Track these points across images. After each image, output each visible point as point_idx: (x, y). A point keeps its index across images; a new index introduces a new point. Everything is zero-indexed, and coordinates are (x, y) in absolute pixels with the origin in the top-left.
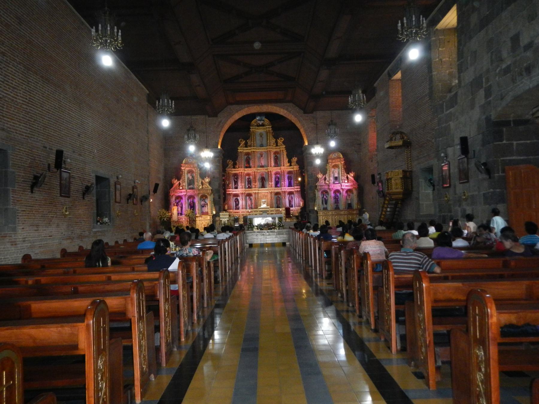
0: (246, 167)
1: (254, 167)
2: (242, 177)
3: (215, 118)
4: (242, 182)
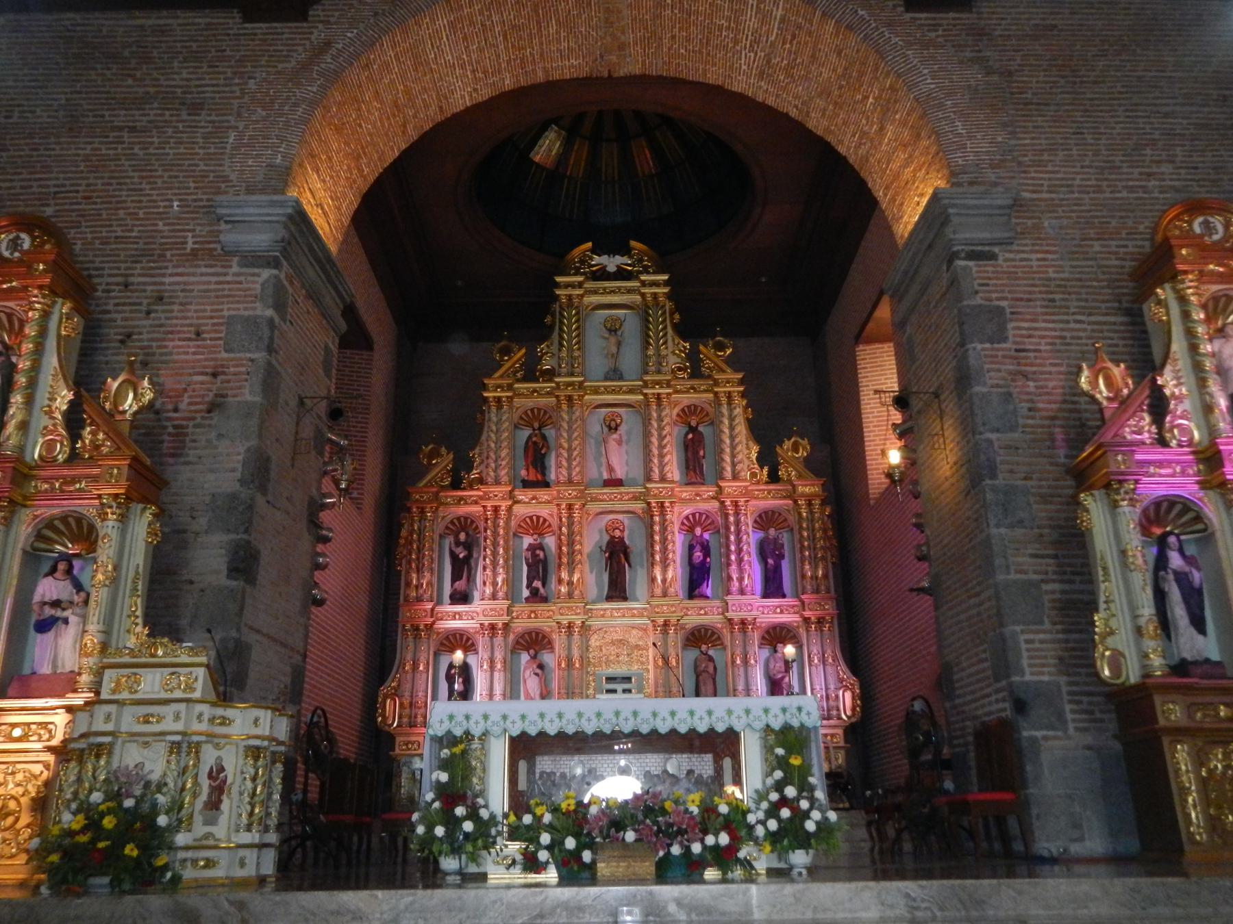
0: (527, 484)
1: (570, 482)
2: (495, 534)
3: (286, 29)
4: (495, 564)
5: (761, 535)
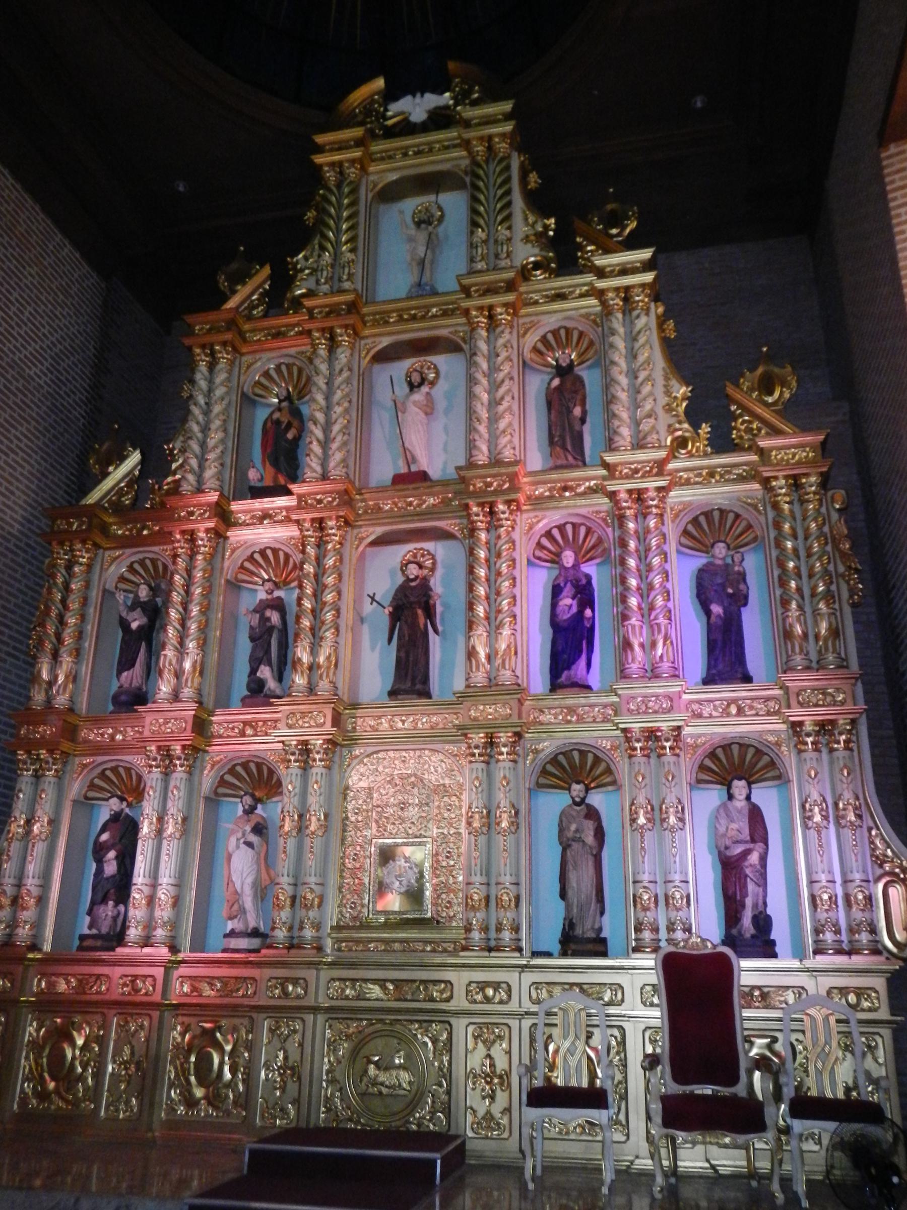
5: (700, 561)
